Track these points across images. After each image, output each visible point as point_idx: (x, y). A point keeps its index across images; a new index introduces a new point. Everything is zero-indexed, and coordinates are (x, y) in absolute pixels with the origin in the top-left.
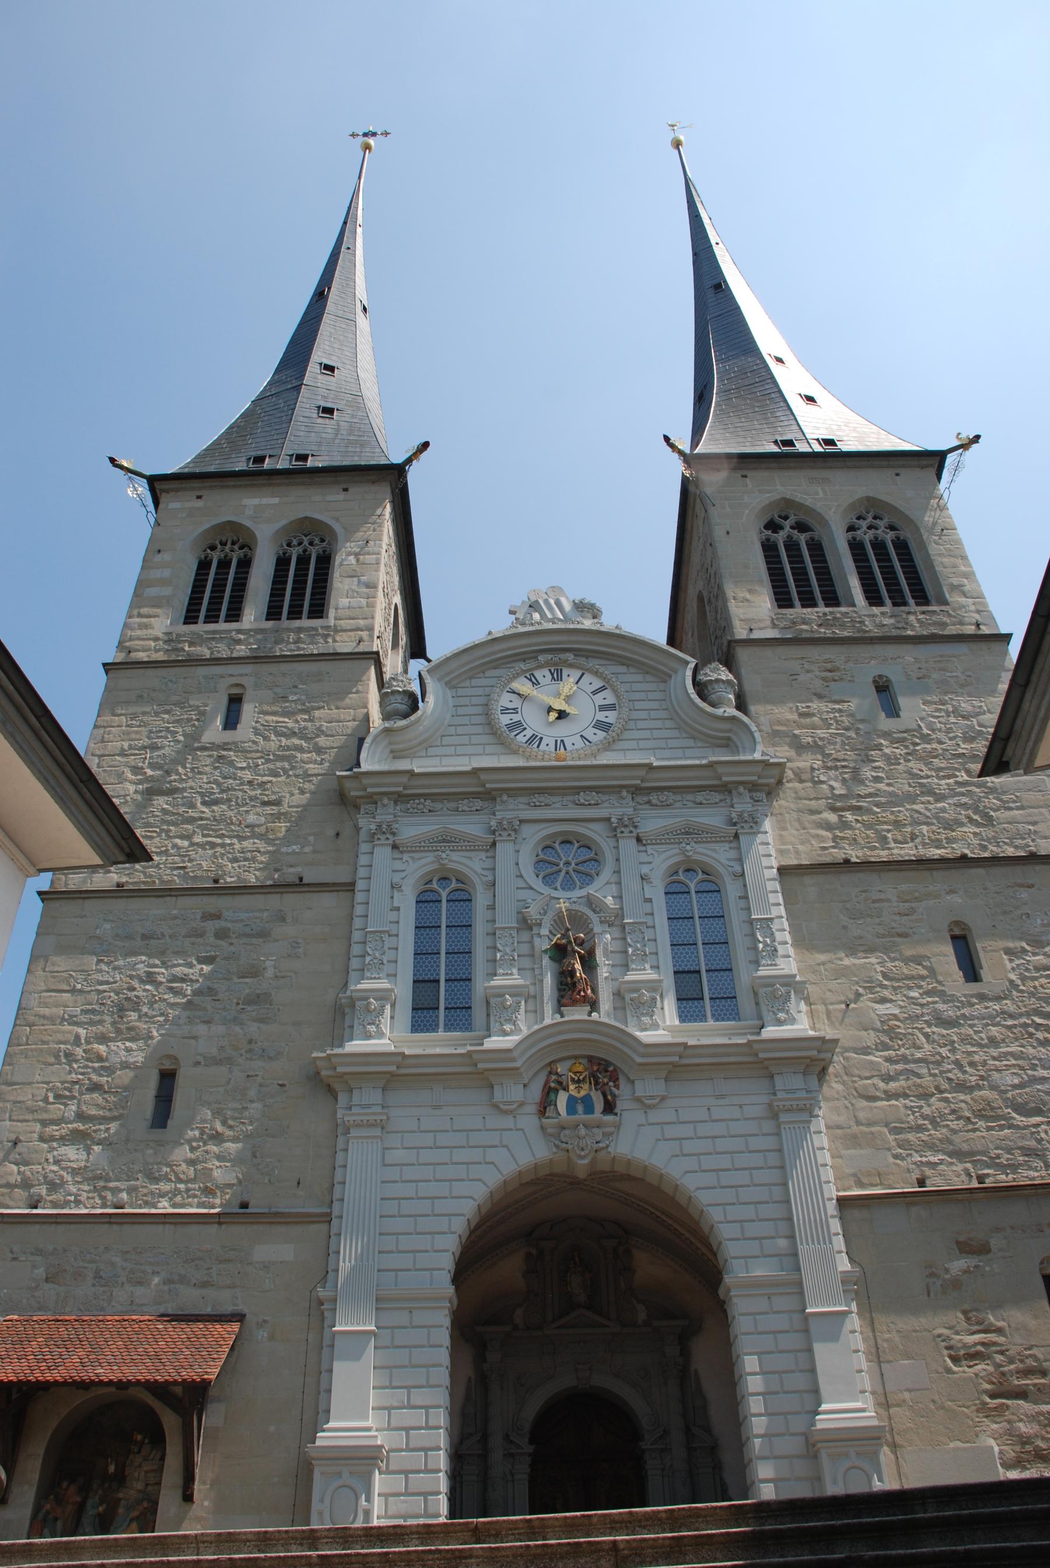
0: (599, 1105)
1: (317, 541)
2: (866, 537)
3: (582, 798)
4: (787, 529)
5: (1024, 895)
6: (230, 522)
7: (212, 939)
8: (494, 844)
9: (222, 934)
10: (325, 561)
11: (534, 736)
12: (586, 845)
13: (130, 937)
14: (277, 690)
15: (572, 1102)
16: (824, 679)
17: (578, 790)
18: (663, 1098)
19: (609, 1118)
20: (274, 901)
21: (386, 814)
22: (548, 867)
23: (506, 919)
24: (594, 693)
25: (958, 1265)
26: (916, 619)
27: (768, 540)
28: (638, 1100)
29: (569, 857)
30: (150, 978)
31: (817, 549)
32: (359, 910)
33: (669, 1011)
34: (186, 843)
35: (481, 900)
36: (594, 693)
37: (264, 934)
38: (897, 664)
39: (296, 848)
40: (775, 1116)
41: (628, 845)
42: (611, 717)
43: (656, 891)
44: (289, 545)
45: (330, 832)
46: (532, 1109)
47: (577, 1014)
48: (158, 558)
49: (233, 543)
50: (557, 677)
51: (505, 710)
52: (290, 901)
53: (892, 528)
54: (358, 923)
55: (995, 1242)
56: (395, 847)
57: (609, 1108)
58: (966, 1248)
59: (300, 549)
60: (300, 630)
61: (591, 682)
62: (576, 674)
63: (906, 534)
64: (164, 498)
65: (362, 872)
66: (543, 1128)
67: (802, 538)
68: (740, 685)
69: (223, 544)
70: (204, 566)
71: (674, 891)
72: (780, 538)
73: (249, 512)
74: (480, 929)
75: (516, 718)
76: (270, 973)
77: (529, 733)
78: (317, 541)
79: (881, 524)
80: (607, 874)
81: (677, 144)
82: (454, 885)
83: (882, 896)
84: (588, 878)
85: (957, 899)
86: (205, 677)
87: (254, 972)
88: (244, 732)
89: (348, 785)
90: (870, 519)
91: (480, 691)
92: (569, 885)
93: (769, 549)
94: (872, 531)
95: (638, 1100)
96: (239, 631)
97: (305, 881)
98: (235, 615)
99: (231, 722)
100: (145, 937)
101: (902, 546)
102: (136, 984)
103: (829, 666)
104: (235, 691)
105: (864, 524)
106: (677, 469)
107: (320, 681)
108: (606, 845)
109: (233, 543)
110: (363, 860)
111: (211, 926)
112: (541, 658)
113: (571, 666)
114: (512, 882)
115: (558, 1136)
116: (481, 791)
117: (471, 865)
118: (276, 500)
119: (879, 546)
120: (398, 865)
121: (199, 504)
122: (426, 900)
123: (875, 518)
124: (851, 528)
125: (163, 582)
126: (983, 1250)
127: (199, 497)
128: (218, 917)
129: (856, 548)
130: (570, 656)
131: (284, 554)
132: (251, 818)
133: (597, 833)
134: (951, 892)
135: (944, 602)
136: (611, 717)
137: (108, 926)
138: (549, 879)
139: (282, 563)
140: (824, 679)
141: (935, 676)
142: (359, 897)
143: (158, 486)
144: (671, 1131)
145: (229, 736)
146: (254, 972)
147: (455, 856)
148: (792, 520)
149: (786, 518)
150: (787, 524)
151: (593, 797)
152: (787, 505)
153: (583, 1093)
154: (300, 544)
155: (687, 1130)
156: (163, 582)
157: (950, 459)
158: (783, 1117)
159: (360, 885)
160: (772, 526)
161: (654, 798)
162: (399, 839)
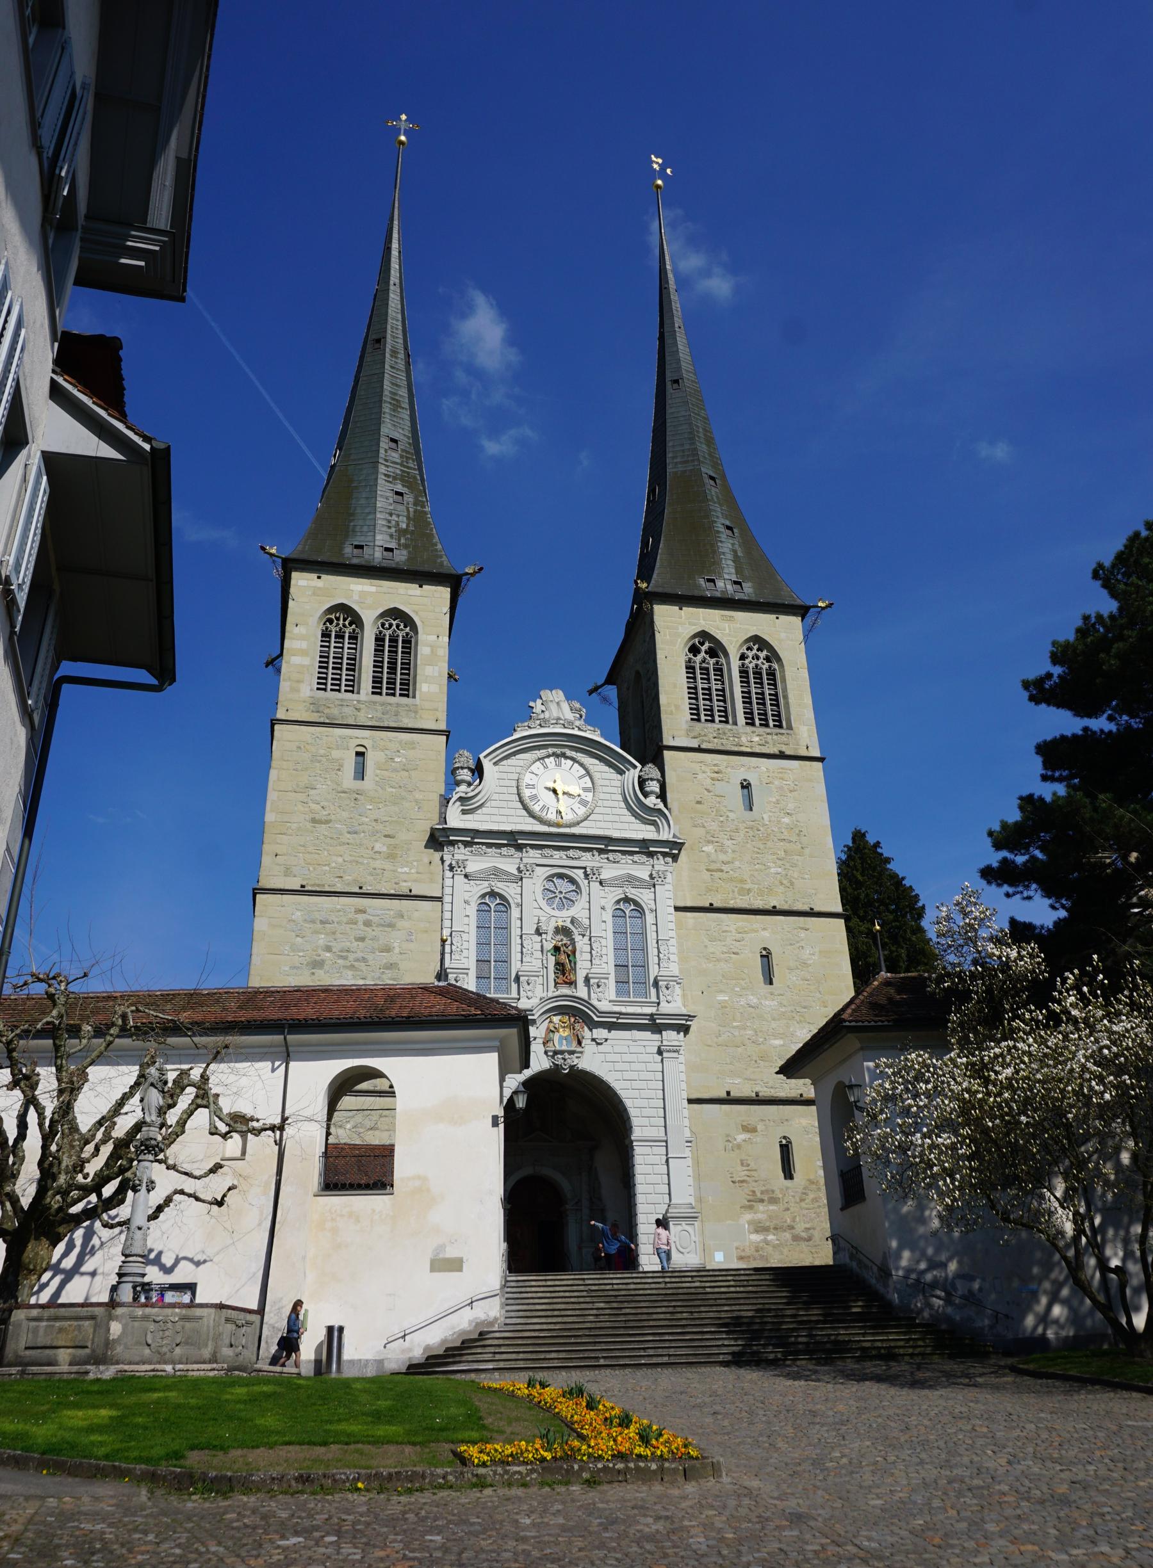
0: (575, 1043)
1: (402, 627)
2: (751, 665)
3: (571, 853)
4: (703, 654)
5: (803, 934)
6: (342, 604)
7: (362, 927)
8: (521, 879)
9: (367, 924)
10: (407, 642)
11: (544, 806)
12: (572, 881)
13: (313, 922)
14: (387, 752)
15: (561, 1038)
16: (713, 779)
17: (569, 848)
18: (606, 1040)
19: (579, 1049)
20: (396, 903)
21: (461, 853)
22: (551, 895)
23: (530, 928)
24: (581, 777)
25: (741, 1137)
26: (770, 740)
27: (690, 659)
28: (593, 1040)
30: (328, 949)
31: (719, 670)
32: (447, 915)
33: (611, 989)
34: (340, 860)
35: (515, 913)
36: (581, 777)
37: (391, 925)
38: (758, 771)
39: (406, 869)
40: (660, 1052)
41: (595, 886)
42: (589, 797)
43: (608, 916)
44: (383, 625)
45: (426, 861)
46: (541, 1041)
47: (565, 990)
48: (296, 630)
49: (345, 620)
50: (559, 765)
51: (528, 786)
52: (406, 903)
53: (768, 659)
54: (447, 923)
55: (760, 1127)
56: (466, 876)
57: (580, 1043)
58: (747, 1129)
59: (390, 631)
60: (398, 705)
61: (578, 770)
62: (569, 762)
63: (775, 666)
64: (295, 575)
65: (448, 891)
66: (546, 1053)
67: (712, 661)
68: (663, 775)
69: (338, 619)
70: (326, 635)
71: (619, 914)
73: (356, 597)
74: (515, 932)
75: (534, 792)
76: (397, 950)
77: (541, 803)
78: (402, 627)
79: (763, 654)
80: (582, 903)
82: (498, 901)
83: (727, 929)
85: (766, 934)
86: (340, 737)
87: (388, 949)
88: (368, 783)
89: (437, 834)
90: (755, 651)
91: (513, 769)
92: (561, 907)
93: (690, 668)
94: (755, 662)
95: (593, 1040)
96: (359, 701)
97: (413, 893)
98: (353, 687)
99: (360, 774)
100: (322, 922)
101: (771, 674)
102: (320, 952)
103: (716, 769)
104: (361, 749)
105: (750, 654)
107: (414, 748)
108: (583, 883)
109: (345, 620)
110: (448, 882)
111: (361, 917)
112: (551, 750)
113: (567, 758)
114: (533, 906)
115: (553, 1057)
116: (513, 840)
117: (510, 890)
118: (373, 589)
119: (758, 673)
120: (467, 888)
121: (320, 583)
122: (483, 909)
124: (743, 657)
125: (303, 653)
126: (754, 1130)
127: (319, 577)
128: (365, 912)
129: (744, 672)
130: (569, 753)
131: (380, 632)
132: (378, 847)
133: (578, 875)
134: (764, 929)
135: (790, 727)
136: (589, 797)
137: (299, 913)
138: (550, 901)
139: (379, 639)
140: (713, 779)
141: (776, 783)
142: (447, 907)
143: (290, 565)
144: (610, 1057)
145: (359, 782)
146: (388, 949)
147: (500, 884)
148: (707, 645)
149: (702, 644)
150: (704, 648)
151: (579, 853)
152: (704, 635)
153: (566, 1034)
154: (391, 625)
155: (617, 1057)
156: (303, 653)
157: (812, 610)
158: (665, 1055)
159: (447, 899)
160: (694, 650)
161: (611, 856)
162: (468, 870)
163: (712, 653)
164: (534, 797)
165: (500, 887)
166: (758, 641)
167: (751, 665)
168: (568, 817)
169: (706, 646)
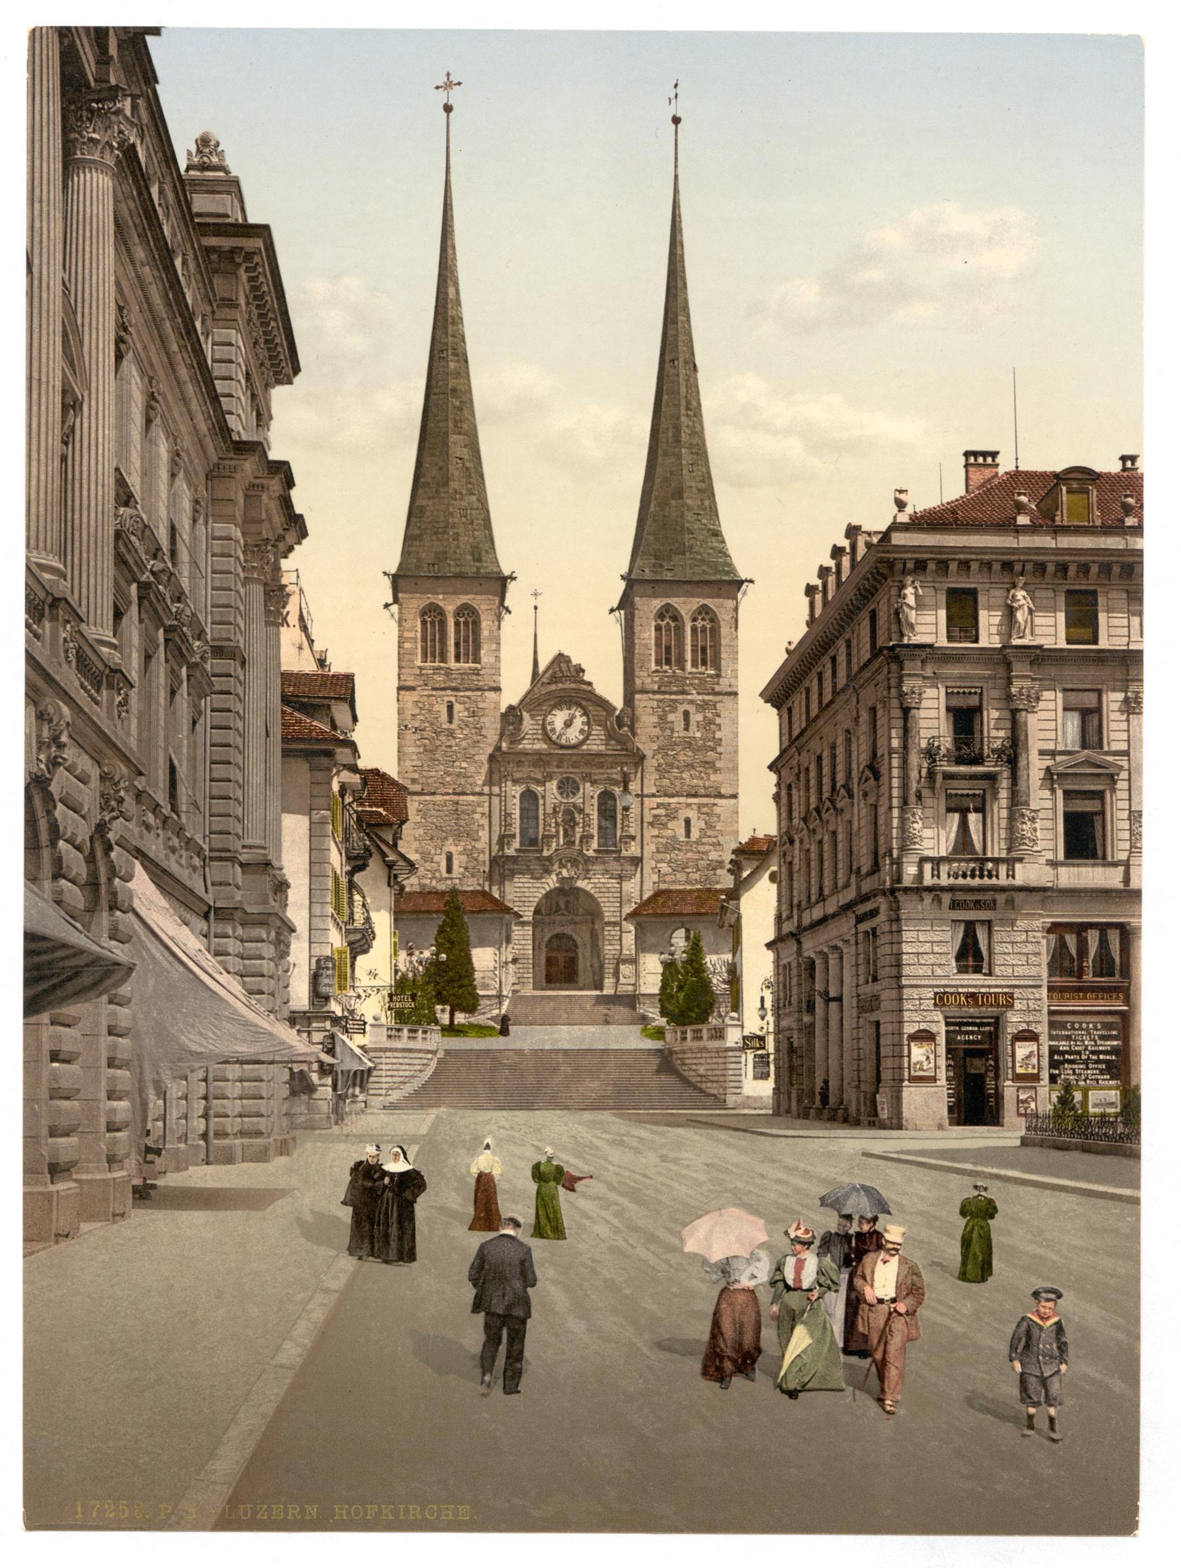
12: (574, 781)
29: (568, 786)
41: (588, 785)
53: (712, 620)
67: (673, 624)
72: (663, 624)
79: (707, 617)
81: (676, 120)
84: (574, 794)
106: (622, 585)
116: (539, 759)
123: (707, 613)
124: (694, 620)
129: (694, 629)
139: (457, 624)
149: (667, 611)
163: (675, 618)
164: (553, 730)
165: (533, 787)
166: (704, 610)
167: (699, 624)
168: (574, 741)
169: (666, 612)
